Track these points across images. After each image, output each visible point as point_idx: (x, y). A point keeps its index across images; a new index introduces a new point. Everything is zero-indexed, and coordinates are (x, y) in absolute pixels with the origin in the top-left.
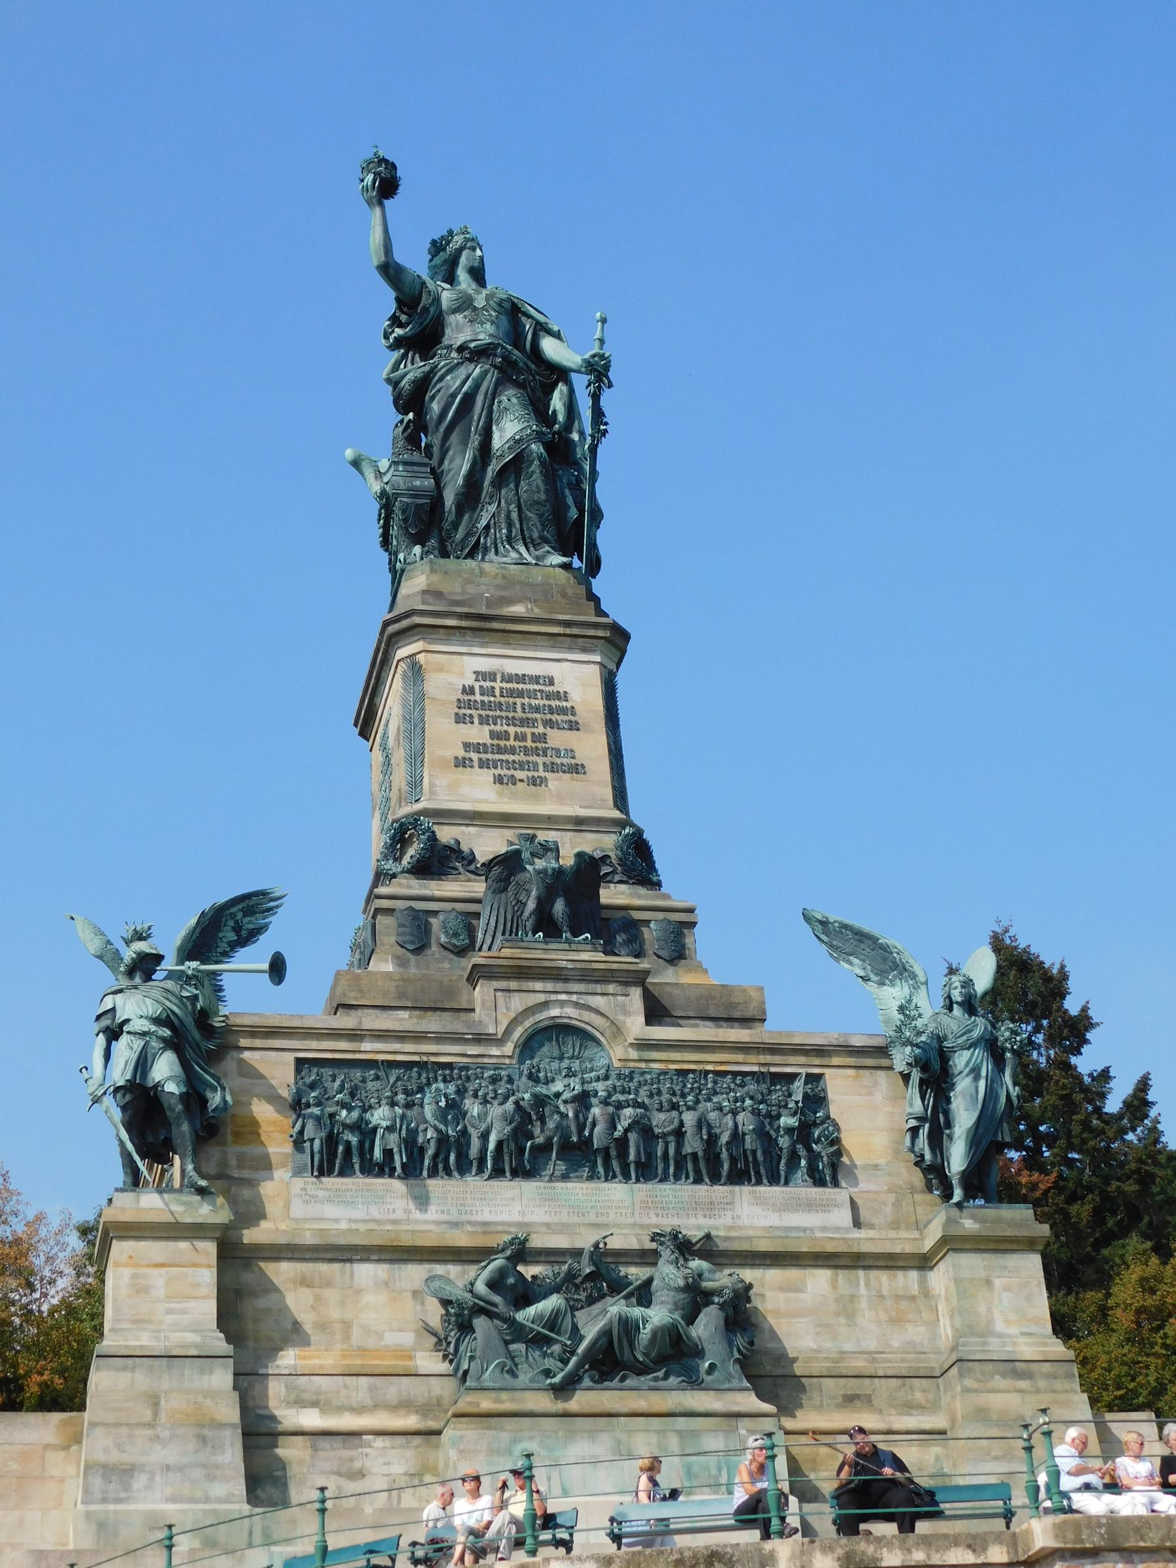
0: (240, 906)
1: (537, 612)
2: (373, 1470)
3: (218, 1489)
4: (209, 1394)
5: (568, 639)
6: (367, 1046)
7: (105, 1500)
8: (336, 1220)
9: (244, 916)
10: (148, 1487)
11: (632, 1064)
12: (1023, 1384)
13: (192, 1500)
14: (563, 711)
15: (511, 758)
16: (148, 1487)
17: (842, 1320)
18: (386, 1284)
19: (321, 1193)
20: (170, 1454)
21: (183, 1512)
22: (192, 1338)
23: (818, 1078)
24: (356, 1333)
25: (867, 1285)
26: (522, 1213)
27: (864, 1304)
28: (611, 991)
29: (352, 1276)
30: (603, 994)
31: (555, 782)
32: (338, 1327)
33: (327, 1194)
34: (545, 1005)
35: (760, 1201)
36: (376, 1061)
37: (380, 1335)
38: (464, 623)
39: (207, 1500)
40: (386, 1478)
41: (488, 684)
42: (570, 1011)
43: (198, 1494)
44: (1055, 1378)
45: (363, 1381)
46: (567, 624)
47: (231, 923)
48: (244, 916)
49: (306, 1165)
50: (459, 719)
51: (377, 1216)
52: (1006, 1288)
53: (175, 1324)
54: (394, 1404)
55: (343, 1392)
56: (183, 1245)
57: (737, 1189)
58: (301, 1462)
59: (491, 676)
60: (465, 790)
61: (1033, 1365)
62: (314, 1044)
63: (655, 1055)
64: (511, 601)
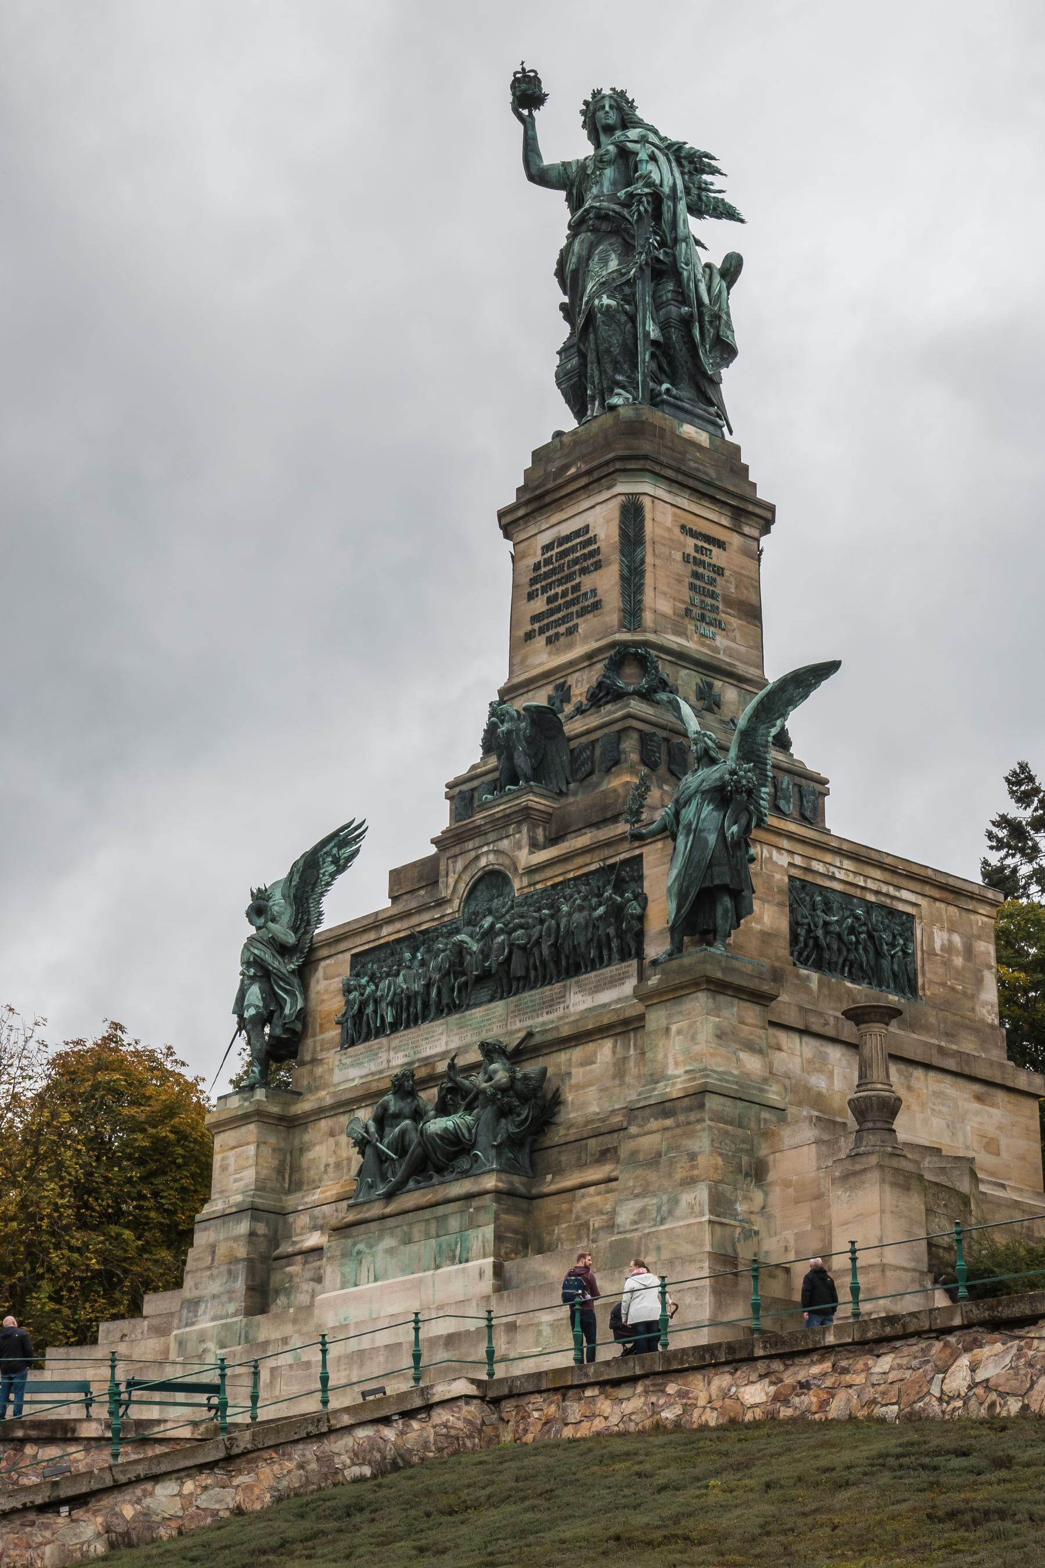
0: (332, 844)
1: (584, 468)
4: (236, 1239)
5: (595, 485)
6: (385, 931)
8: (353, 1080)
9: (339, 850)
10: (205, 1312)
11: (526, 890)
12: (669, 1122)
14: (592, 554)
15: (560, 615)
16: (205, 1312)
17: (617, 1082)
19: (348, 1061)
23: (641, 856)
25: (635, 1045)
26: (447, 1043)
27: (632, 1064)
30: (507, 837)
31: (584, 625)
34: (477, 858)
35: (582, 989)
36: (388, 943)
38: (529, 509)
39: (227, 1316)
41: (549, 554)
42: (491, 857)
44: (691, 1110)
46: (589, 472)
47: (330, 859)
48: (339, 850)
50: (531, 596)
51: (374, 1069)
52: (679, 1032)
57: (568, 982)
60: (530, 661)
61: (677, 1102)
62: (358, 941)
63: (537, 877)
64: (566, 467)
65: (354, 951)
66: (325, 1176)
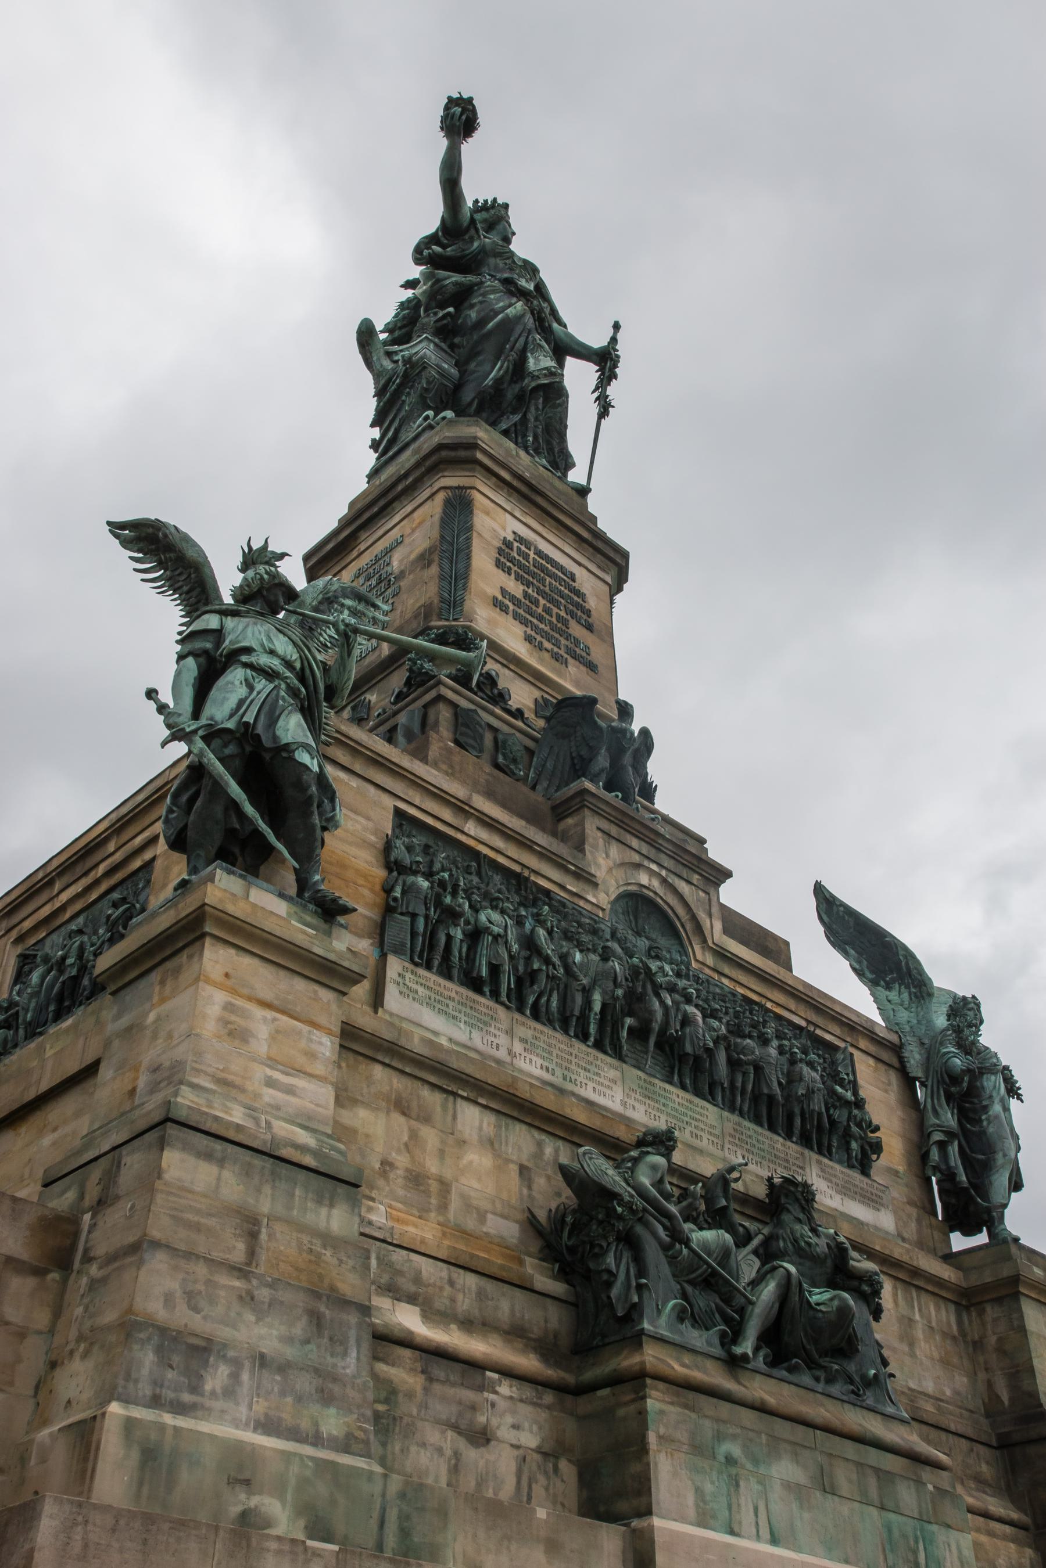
2: (499, 1433)
3: (333, 1423)
5: (591, 550)
7: (155, 1402)
13: (294, 1434)
16: (229, 1393)
18: (492, 1144)
19: (421, 990)
20: (267, 1334)
21: (287, 1456)
22: (304, 1137)
24: (455, 1203)
28: (695, 882)
29: (454, 1117)
32: (434, 1186)
33: (428, 993)
34: (638, 866)
37: (482, 1218)
38: (515, 483)
40: (516, 1452)
42: (656, 884)
43: (305, 1424)
45: (471, 1281)
49: (403, 945)
53: (278, 1108)
54: (506, 1327)
55: (448, 1289)
56: (300, 985)
58: (410, 1395)
59: (528, 544)
65: (402, 806)
66: (381, 1182)
